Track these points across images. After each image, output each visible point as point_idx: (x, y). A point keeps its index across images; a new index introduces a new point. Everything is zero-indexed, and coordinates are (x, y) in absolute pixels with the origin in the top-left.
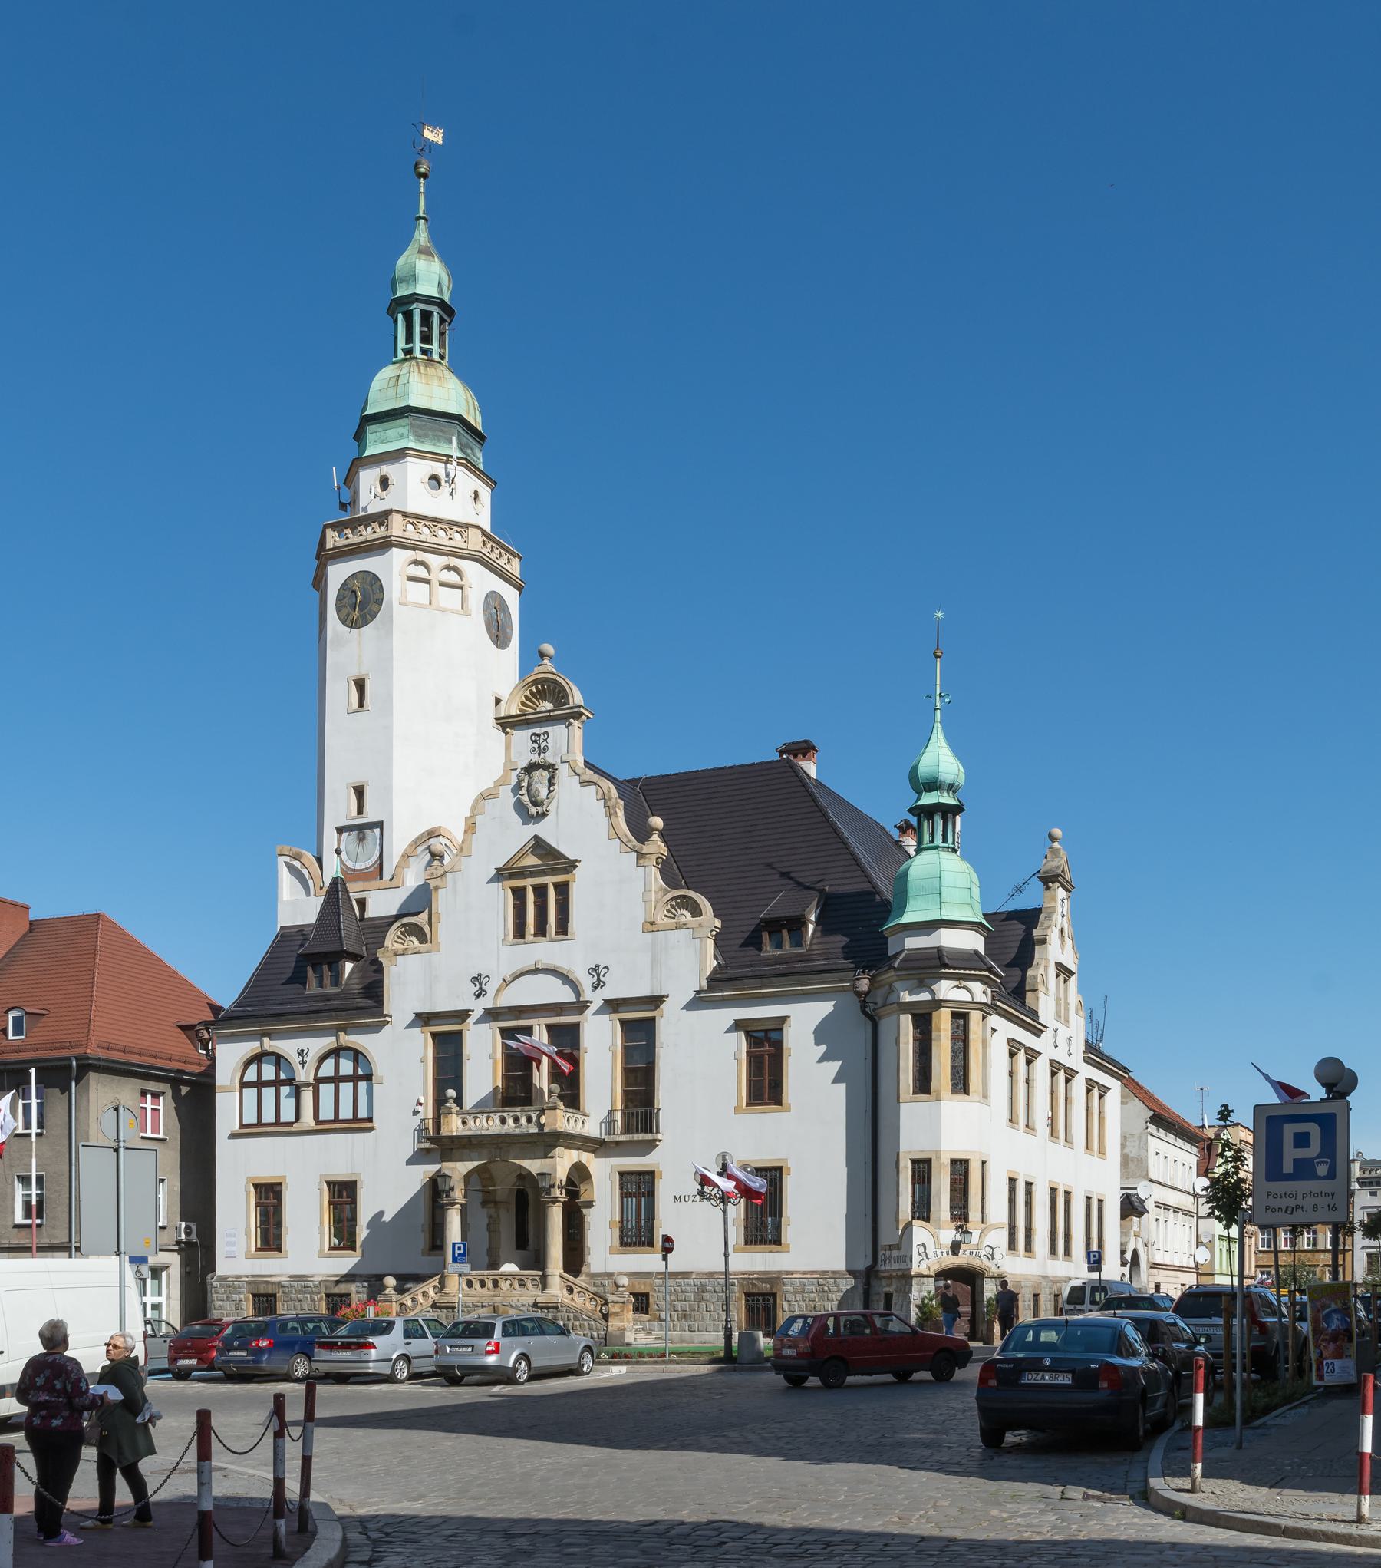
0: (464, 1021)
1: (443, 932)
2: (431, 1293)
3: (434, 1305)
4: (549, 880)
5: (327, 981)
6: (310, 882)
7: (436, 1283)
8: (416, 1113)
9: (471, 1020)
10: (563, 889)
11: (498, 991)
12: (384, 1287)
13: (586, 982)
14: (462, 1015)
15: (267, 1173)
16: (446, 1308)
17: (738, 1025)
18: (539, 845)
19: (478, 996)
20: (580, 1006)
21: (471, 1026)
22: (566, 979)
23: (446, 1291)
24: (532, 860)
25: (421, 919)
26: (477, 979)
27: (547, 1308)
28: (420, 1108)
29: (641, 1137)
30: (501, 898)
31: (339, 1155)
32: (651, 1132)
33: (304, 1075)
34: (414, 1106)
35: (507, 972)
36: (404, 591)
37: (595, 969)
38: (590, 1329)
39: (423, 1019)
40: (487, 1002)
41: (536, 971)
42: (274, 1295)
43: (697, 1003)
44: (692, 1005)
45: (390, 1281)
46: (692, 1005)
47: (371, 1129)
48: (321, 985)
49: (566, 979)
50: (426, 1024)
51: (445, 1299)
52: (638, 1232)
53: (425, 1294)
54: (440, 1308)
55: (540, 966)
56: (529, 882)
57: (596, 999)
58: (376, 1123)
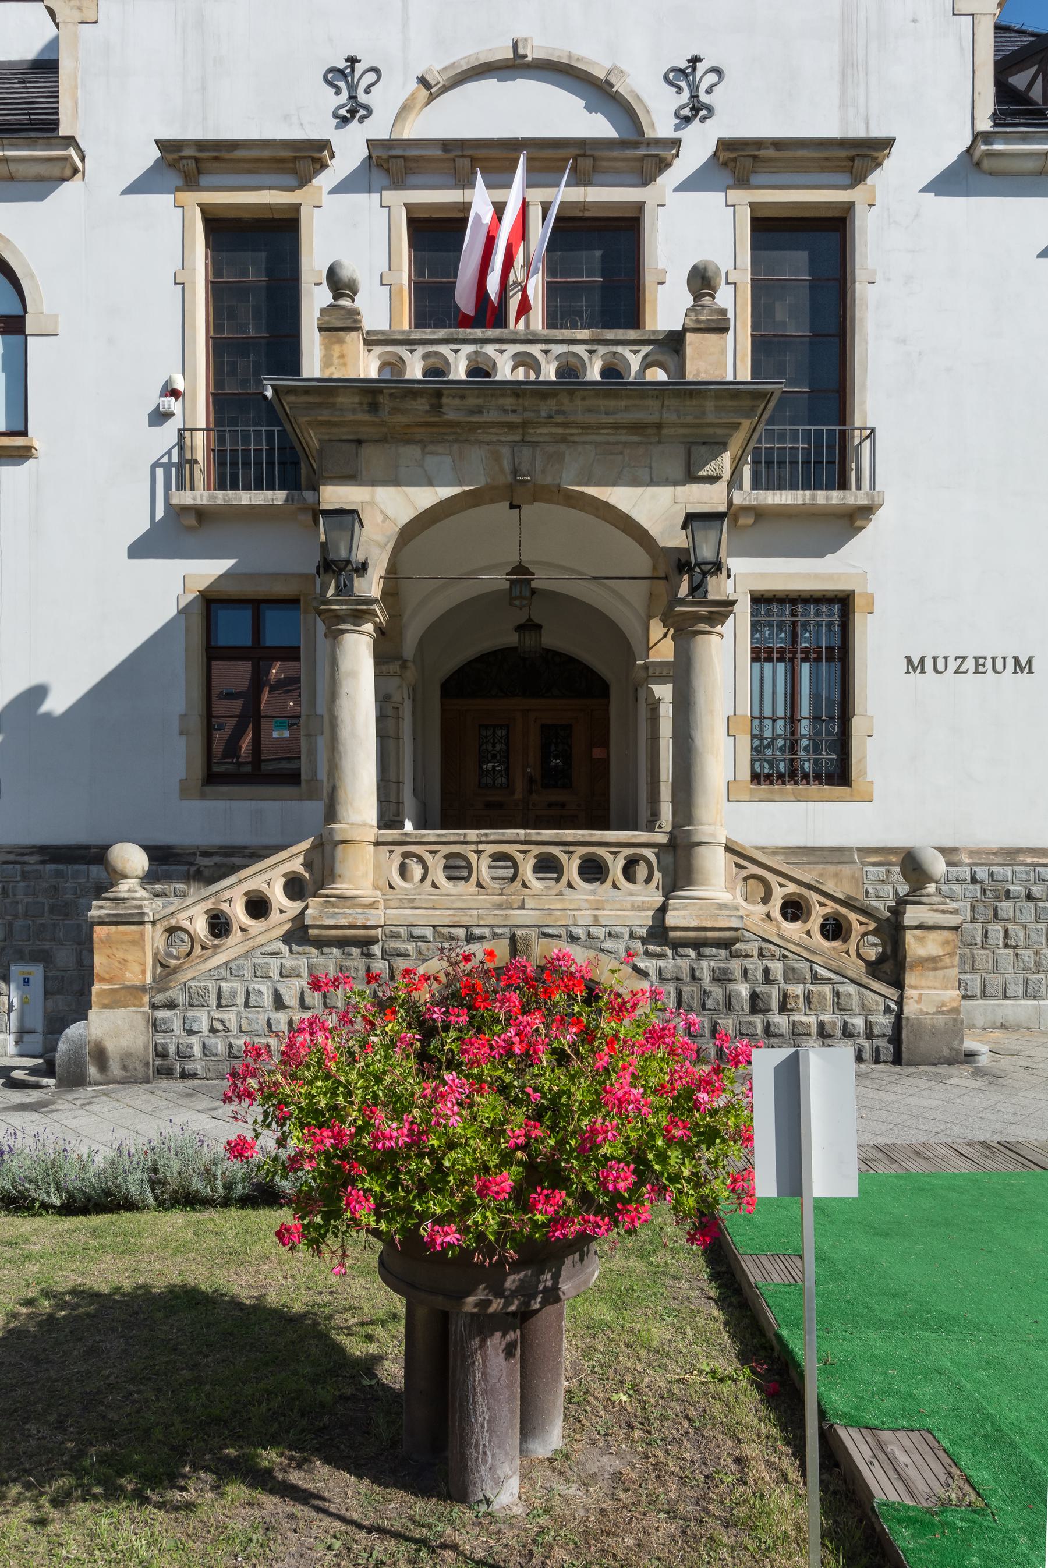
0: (304, 181)
2: (277, 895)
3: (299, 934)
7: (296, 865)
8: (159, 417)
9: (325, 180)
11: (405, 109)
12: (116, 876)
14: (303, 159)
16: (342, 943)
19: (344, 121)
20: (646, 158)
21: (326, 199)
22: (599, 91)
23: (342, 887)
26: (342, 74)
27: (697, 945)
28: (174, 405)
29: (821, 497)
32: (844, 485)
34: (152, 399)
35: (434, 65)
38: (839, 1004)
39: (185, 162)
40: (379, 127)
43: (972, 173)
44: (950, 182)
45: (132, 858)
46: (950, 182)
47: (24, 454)
50: (190, 183)
51: (344, 916)
53: (258, 907)
54: (320, 944)
55: (532, 52)
57: (697, 146)
58: (36, 436)
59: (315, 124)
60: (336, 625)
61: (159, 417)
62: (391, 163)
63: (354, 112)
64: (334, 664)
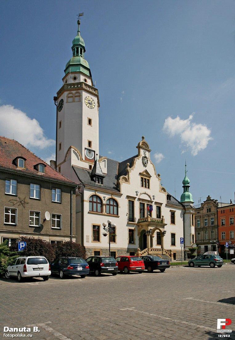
1: (131, 180)
4: (147, 178)
5: (100, 182)
6: (79, 157)
10: (148, 180)
13: (152, 198)
14: (135, 198)
15: (97, 223)
17: (170, 211)
18: (146, 171)
24: (144, 173)
25: (126, 177)
30: (139, 178)
31: (114, 221)
33: (104, 202)
35: (142, 192)
36: (67, 100)
37: (153, 196)
41: (145, 193)
42: (100, 252)
48: (99, 183)
49: (149, 196)
52: (160, 242)
56: (144, 177)
59: (135, 196)
60: (148, 235)
61: (127, 215)
62: (139, 199)
63: (137, 195)
64: (162, 239)
